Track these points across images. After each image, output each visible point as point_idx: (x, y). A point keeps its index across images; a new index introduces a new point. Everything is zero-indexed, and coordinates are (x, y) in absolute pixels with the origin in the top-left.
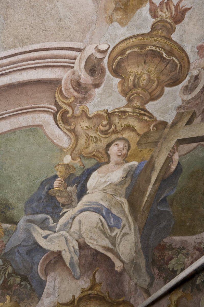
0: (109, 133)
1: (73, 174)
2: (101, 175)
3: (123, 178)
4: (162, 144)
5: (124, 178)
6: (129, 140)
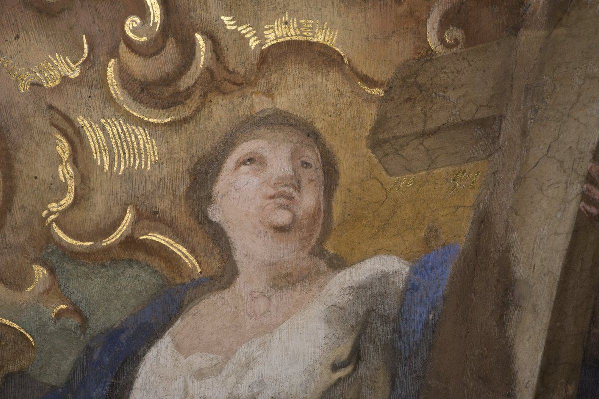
0: (189, 93)
1: (22, 373)
2: (198, 360)
3: (335, 368)
4: (524, 133)
5: (344, 365)
6: (318, 125)
